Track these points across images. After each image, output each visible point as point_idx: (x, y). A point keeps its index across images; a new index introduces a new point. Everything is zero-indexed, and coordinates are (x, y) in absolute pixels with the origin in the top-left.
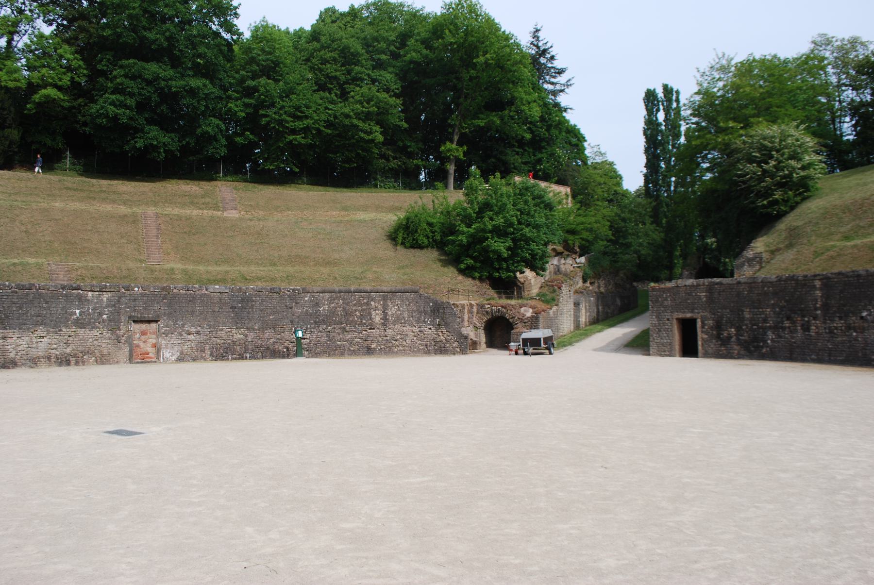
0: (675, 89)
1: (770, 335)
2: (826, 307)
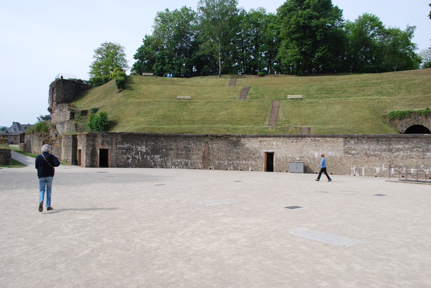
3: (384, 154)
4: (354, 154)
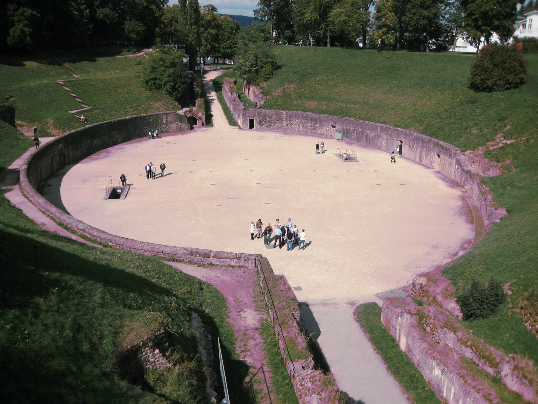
1: (273, 124)
2: (286, 119)
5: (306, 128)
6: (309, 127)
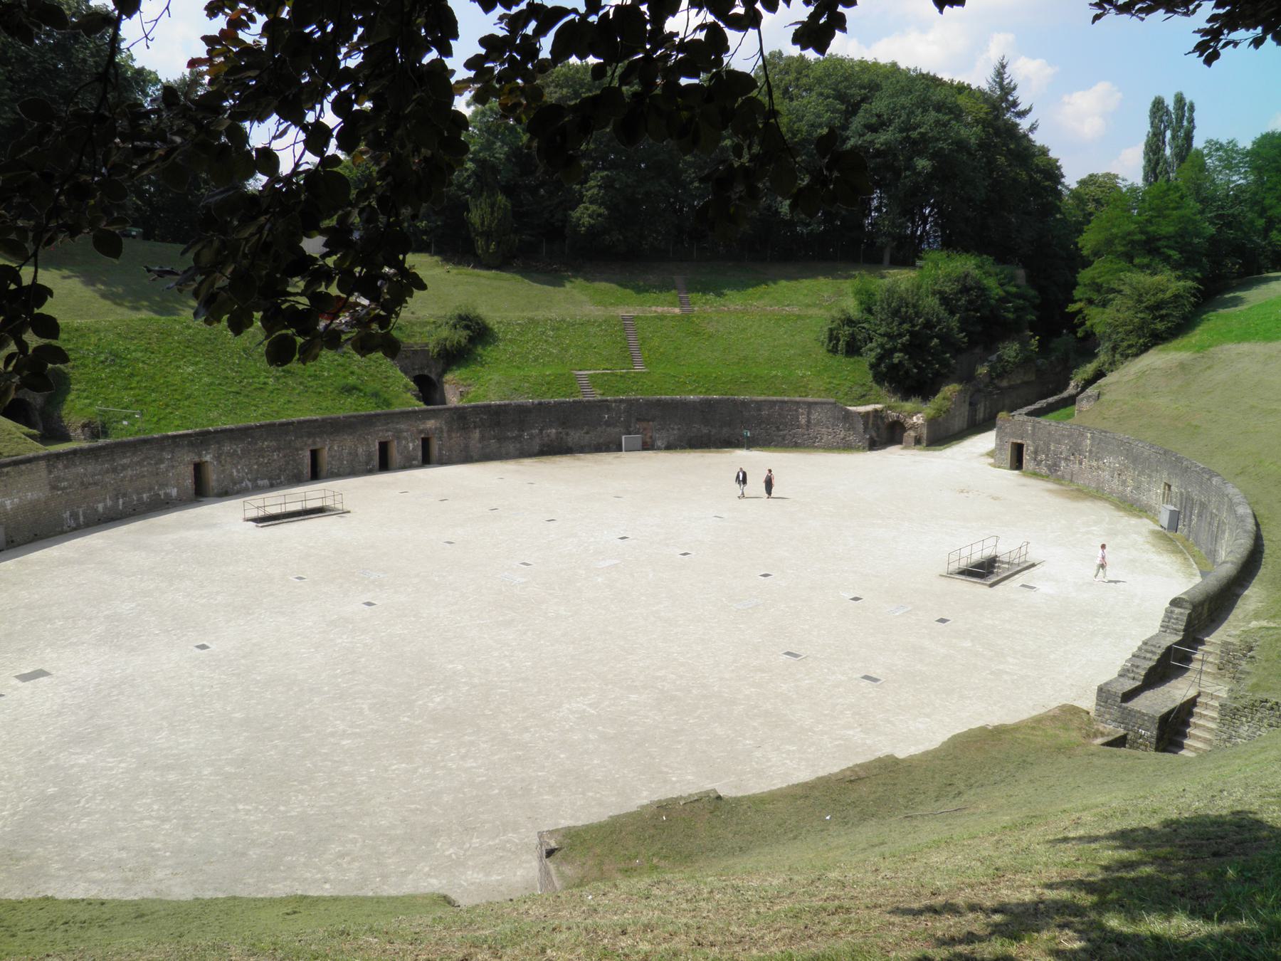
0: (1187, 101)
3: (109, 478)
4: (64, 489)
5: (1124, 483)
6: (1130, 481)
